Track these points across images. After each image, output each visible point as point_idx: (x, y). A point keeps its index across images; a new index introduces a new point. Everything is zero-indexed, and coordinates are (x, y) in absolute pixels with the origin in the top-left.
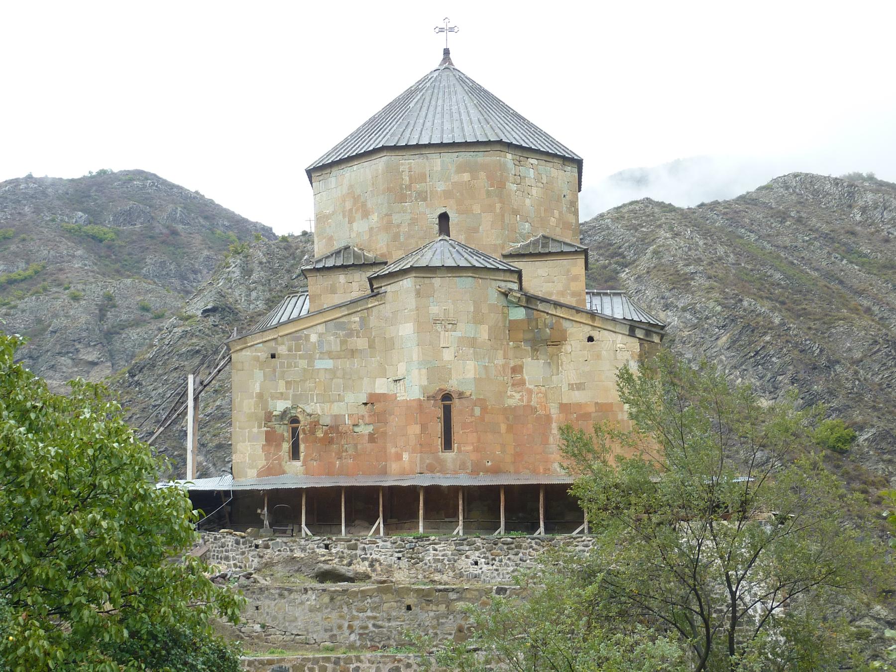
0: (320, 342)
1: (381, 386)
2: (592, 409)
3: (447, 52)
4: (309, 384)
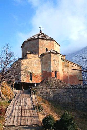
0: (35, 62)
2: (73, 76)
3: (41, 31)
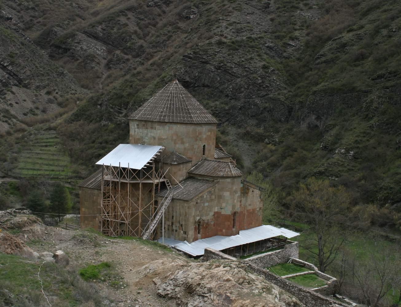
1: (216, 209)
4: (204, 211)
